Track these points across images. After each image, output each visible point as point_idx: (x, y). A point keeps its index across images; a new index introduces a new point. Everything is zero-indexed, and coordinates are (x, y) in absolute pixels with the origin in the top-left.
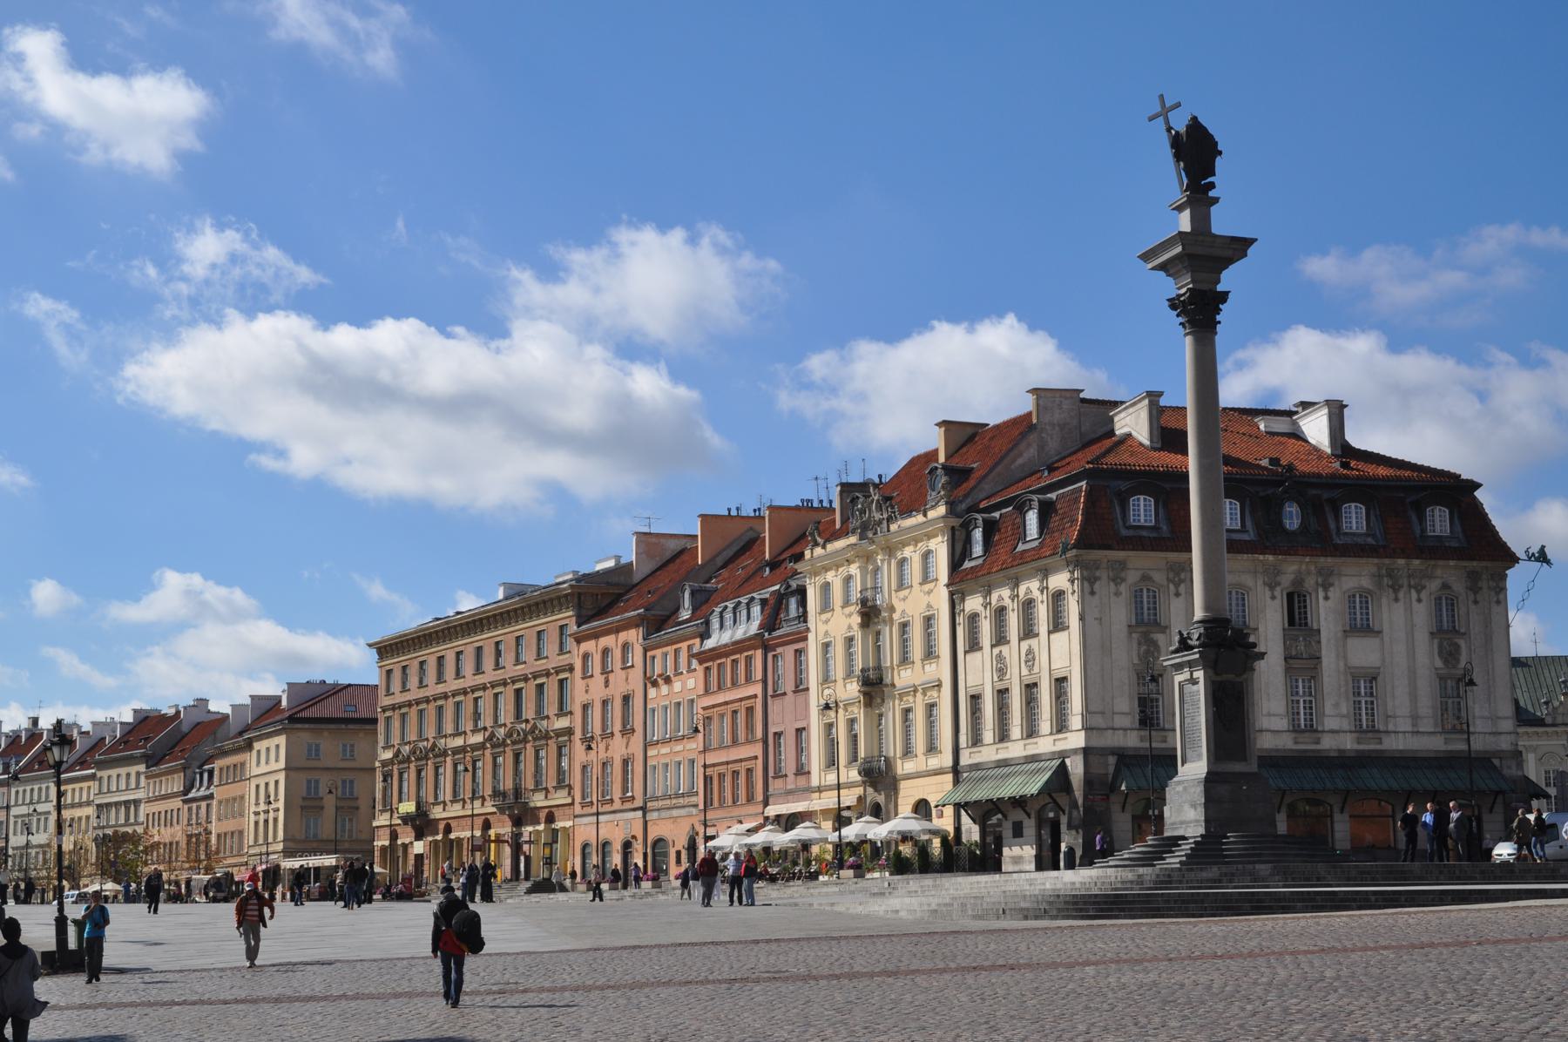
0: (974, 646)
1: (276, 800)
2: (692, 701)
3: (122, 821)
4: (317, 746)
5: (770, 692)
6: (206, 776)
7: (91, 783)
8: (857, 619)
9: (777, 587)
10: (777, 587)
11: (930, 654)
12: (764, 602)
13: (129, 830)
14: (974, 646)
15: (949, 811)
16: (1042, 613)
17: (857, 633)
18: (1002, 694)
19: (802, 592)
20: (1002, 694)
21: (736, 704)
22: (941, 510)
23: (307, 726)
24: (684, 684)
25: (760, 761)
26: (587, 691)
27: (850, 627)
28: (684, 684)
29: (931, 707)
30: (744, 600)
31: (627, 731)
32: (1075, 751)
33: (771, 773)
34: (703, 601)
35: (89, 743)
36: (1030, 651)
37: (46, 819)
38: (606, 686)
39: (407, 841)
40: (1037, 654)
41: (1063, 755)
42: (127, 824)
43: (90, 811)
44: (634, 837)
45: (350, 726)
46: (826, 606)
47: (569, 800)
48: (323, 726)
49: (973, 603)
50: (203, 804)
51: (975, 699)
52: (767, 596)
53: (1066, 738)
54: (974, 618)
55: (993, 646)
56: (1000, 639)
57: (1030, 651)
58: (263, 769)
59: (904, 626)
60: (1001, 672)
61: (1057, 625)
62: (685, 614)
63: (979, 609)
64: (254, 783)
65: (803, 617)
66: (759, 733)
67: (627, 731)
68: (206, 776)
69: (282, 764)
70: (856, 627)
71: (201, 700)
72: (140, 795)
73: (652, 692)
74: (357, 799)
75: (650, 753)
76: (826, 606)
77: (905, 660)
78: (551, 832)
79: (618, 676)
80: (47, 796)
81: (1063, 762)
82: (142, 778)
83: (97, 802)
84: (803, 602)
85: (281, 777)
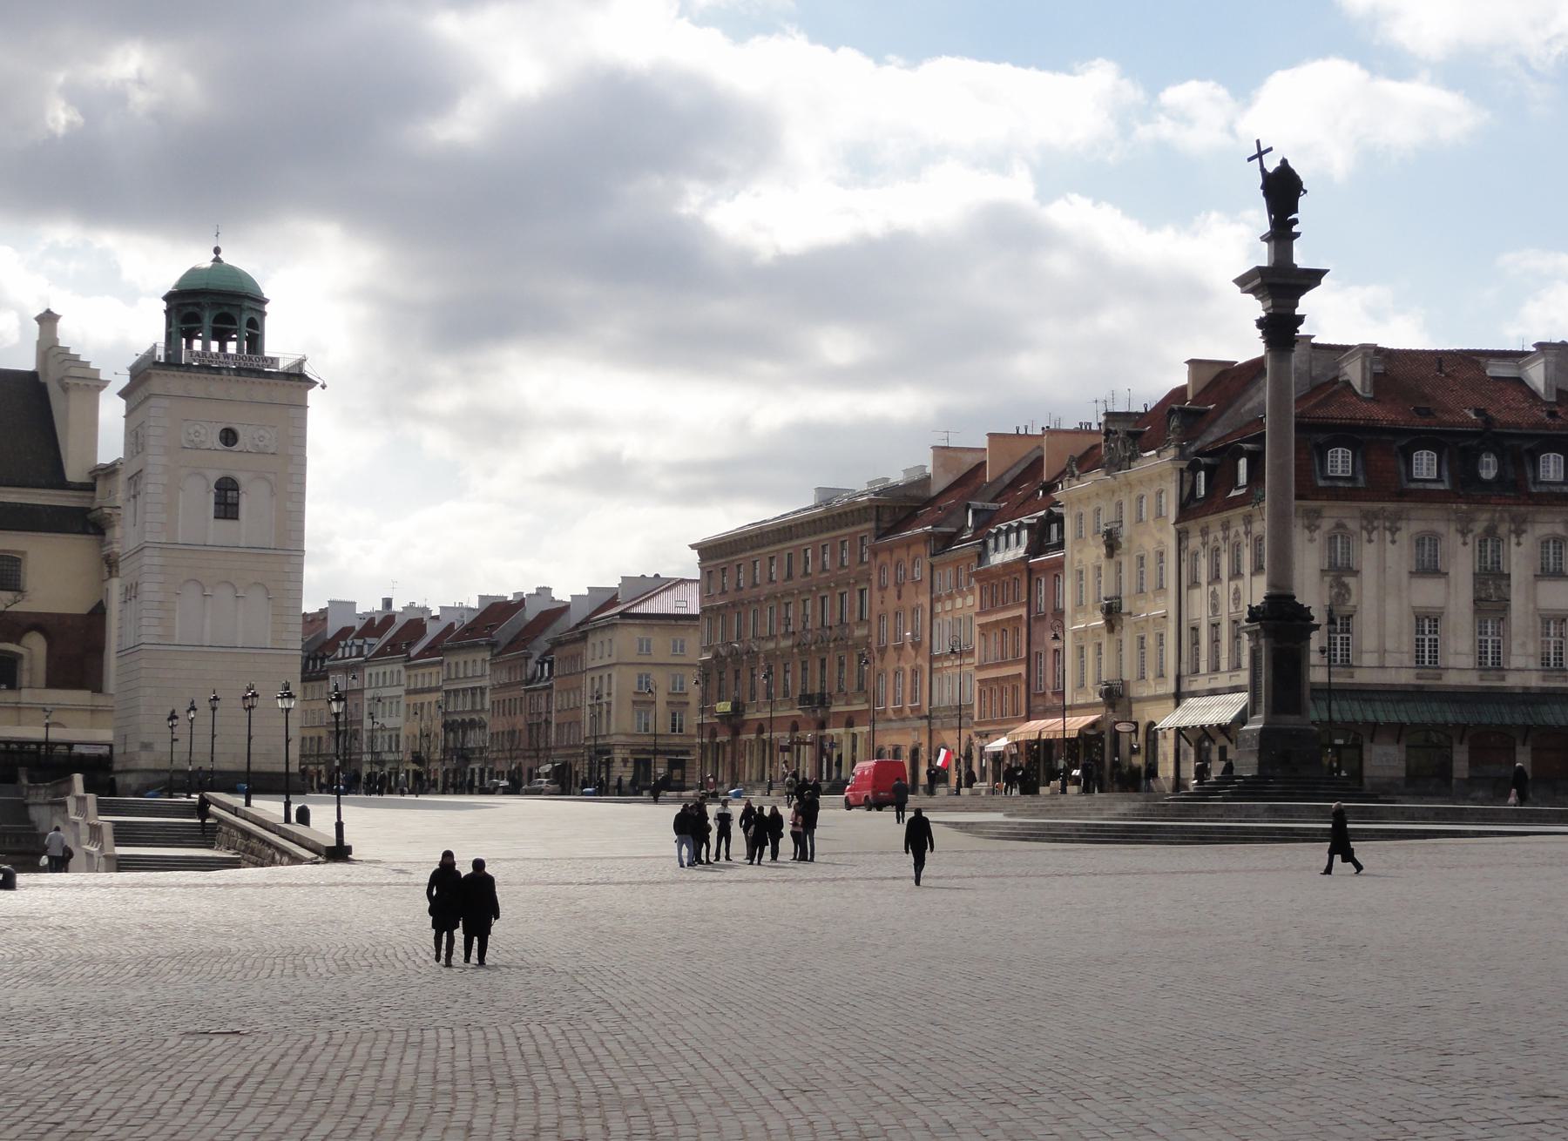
0: (1195, 584)
3: (468, 707)
4: (649, 641)
7: (439, 669)
8: (1104, 550)
12: (1030, 527)
13: (475, 717)
14: (1195, 584)
17: (1103, 562)
18: (1215, 626)
19: (1060, 519)
20: (1215, 626)
23: (637, 622)
26: (882, 602)
27: (1098, 557)
34: (986, 519)
37: (398, 702)
42: (473, 711)
43: (439, 696)
45: (680, 622)
46: (1079, 536)
48: (654, 622)
50: (544, 694)
51: (1195, 629)
54: (1195, 554)
55: (1209, 584)
56: (1215, 578)
60: (1215, 608)
64: (589, 676)
70: (1103, 557)
71: (545, 588)
72: (486, 682)
74: (687, 694)
78: (850, 736)
83: (445, 688)
84: (1061, 530)
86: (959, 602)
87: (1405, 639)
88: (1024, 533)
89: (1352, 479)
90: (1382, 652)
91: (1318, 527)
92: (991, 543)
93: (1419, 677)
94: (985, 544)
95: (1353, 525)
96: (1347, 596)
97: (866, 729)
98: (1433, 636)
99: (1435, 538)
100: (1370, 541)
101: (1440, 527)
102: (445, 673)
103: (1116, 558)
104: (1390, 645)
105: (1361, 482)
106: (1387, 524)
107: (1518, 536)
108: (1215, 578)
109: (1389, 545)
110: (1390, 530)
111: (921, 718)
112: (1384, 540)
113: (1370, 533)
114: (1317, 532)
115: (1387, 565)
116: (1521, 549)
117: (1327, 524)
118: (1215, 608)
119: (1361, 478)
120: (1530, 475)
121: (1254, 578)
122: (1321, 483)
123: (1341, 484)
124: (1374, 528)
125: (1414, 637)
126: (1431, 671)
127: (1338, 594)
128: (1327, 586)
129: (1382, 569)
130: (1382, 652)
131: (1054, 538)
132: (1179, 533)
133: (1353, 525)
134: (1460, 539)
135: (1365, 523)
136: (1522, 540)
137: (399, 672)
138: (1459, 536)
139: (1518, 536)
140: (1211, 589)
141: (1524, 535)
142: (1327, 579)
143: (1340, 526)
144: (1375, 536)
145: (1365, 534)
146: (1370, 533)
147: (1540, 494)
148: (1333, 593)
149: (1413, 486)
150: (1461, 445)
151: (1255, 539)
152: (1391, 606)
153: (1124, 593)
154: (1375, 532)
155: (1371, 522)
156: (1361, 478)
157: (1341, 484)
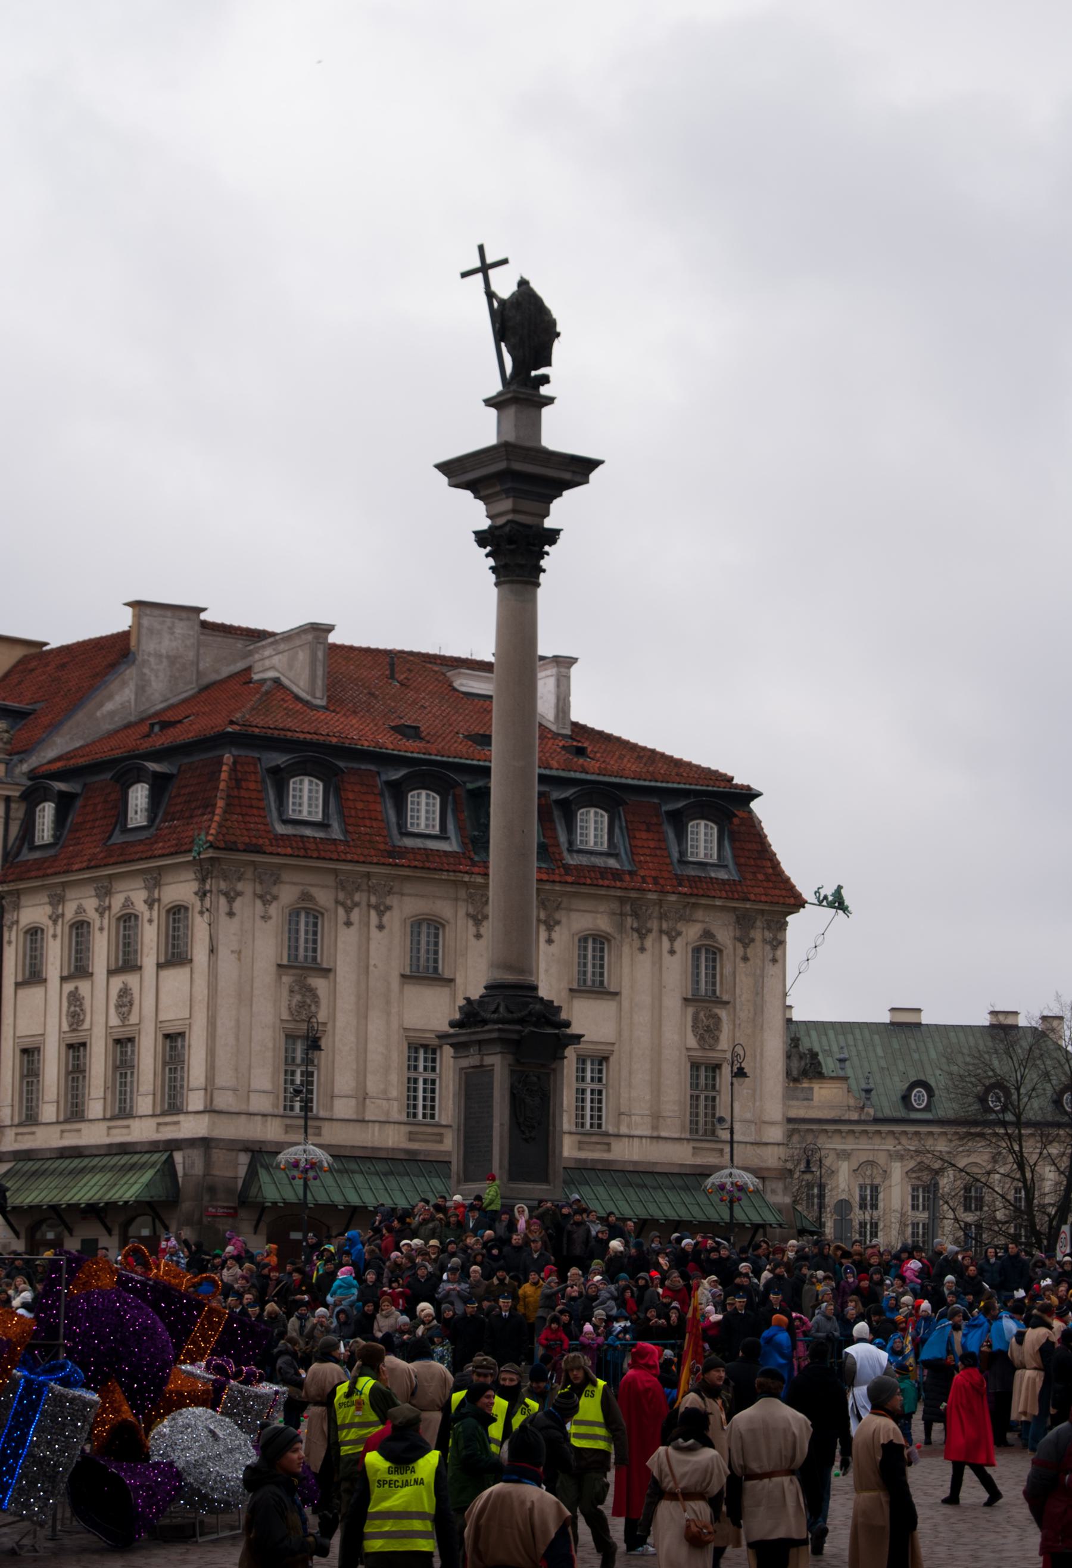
87: (394, 1078)
89: (323, 825)
90: (362, 1097)
91: (275, 898)
93: (412, 1137)
95: (324, 897)
96: (313, 1008)
98: (430, 1076)
99: (435, 925)
100: (348, 924)
101: (444, 909)
104: (373, 1085)
105: (336, 832)
106: (373, 900)
107: (550, 928)
109: (374, 932)
110: (376, 908)
112: (368, 925)
113: (348, 910)
114: (274, 905)
115: (372, 962)
116: (553, 949)
117: (288, 894)
119: (335, 825)
120: (563, 838)
122: (281, 829)
123: (308, 832)
124: (357, 904)
125: (406, 1075)
126: (429, 1130)
127: (302, 1005)
128: (285, 993)
129: (364, 968)
130: (362, 1097)
133: (324, 897)
134: (472, 930)
135: (341, 896)
136: (555, 936)
138: (471, 923)
139: (550, 928)
141: (557, 928)
142: (286, 979)
143: (306, 897)
144: (355, 915)
145: (341, 911)
146: (348, 910)
147: (579, 868)
148: (294, 1002)
149: (409, 842)
150: (470, 786)
152: (376, 1026)
154: (356, 911)
155: (351, 895)
156: (335, 825)
157: (308, 832)
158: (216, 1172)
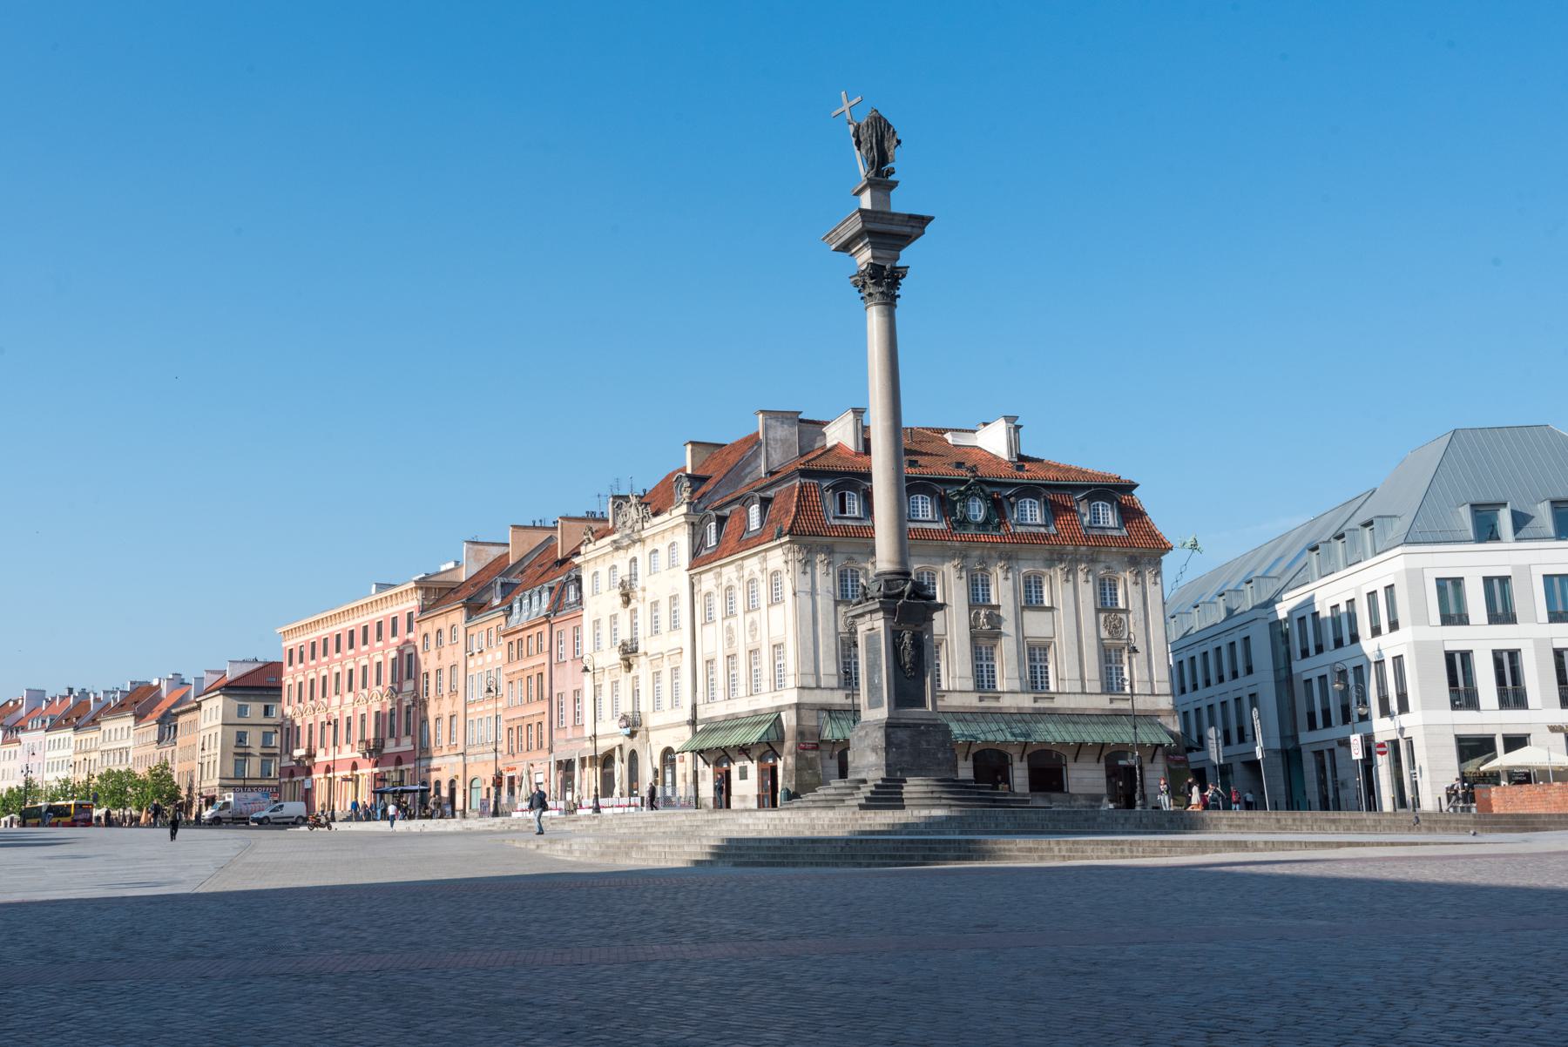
0: (709, 619)
1: (215, 747)
2: (500, 669)
5: (554, 661)
6: (172, 729)
8: (620, 600)
9: (561, 578)
10: (561, 578)
11: (675, 626)
15: (688, 756)
16: (763, 590)
19: (579, 579)
21: (529, 671)
22: (684, 509)
24: (494, 657)
25: (547, 715)
28: (494, 657)
29: (675, 671)
30: (537, 589)
31: (453, 692)
32: (790, 706)
33: (555, 726)
35: (100, 706)
36: (753, 623)
38: (439, 659)
39: (300, 778)
40: (758, 626)
41: (779, 710)
44: (457, 777)
47: (412, 748)
49: (708, 582)
52: (554, 585)
53: (782, 696)
56: (729, 614)
57: (753, 623)
58: (208, 724)
59: (655, 604)
60: (730, 640)
61: (775, 600)
62: (497, 602)
63: (714, 589)
64: (202, 734)
65: (580, 601)
66: (546, 694)
67: (453, 692)
68: (172, 729)
69: (220, 721)
71: (176, 674)
72: (130, 743)
73: (471, 663)
75: (469, 711)
76: (595, 592)
77: (655, 631)
79: (447, 650)
80: (69, 744)
81: (779, 715)
82: (132, 731)
83: (101, 749)
84: (579, 589)
85: (219, 730)
86: (489, 658)
88: (545, 595)
92: (516, 606)
94: (511, 607)
97: (411, 766)
102: (102, 738)
103: (631, 606)
108: (729, 614)
111: (457, 755)
118: (730, 640)
121: (771, 610)
131: (572, 599)
132: (691, 577)
137: (69, 738)
140: (726, 623)
151: (771, 575)
153: (640, 636)
158: (804, 723)
